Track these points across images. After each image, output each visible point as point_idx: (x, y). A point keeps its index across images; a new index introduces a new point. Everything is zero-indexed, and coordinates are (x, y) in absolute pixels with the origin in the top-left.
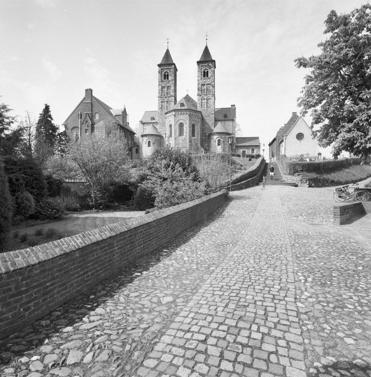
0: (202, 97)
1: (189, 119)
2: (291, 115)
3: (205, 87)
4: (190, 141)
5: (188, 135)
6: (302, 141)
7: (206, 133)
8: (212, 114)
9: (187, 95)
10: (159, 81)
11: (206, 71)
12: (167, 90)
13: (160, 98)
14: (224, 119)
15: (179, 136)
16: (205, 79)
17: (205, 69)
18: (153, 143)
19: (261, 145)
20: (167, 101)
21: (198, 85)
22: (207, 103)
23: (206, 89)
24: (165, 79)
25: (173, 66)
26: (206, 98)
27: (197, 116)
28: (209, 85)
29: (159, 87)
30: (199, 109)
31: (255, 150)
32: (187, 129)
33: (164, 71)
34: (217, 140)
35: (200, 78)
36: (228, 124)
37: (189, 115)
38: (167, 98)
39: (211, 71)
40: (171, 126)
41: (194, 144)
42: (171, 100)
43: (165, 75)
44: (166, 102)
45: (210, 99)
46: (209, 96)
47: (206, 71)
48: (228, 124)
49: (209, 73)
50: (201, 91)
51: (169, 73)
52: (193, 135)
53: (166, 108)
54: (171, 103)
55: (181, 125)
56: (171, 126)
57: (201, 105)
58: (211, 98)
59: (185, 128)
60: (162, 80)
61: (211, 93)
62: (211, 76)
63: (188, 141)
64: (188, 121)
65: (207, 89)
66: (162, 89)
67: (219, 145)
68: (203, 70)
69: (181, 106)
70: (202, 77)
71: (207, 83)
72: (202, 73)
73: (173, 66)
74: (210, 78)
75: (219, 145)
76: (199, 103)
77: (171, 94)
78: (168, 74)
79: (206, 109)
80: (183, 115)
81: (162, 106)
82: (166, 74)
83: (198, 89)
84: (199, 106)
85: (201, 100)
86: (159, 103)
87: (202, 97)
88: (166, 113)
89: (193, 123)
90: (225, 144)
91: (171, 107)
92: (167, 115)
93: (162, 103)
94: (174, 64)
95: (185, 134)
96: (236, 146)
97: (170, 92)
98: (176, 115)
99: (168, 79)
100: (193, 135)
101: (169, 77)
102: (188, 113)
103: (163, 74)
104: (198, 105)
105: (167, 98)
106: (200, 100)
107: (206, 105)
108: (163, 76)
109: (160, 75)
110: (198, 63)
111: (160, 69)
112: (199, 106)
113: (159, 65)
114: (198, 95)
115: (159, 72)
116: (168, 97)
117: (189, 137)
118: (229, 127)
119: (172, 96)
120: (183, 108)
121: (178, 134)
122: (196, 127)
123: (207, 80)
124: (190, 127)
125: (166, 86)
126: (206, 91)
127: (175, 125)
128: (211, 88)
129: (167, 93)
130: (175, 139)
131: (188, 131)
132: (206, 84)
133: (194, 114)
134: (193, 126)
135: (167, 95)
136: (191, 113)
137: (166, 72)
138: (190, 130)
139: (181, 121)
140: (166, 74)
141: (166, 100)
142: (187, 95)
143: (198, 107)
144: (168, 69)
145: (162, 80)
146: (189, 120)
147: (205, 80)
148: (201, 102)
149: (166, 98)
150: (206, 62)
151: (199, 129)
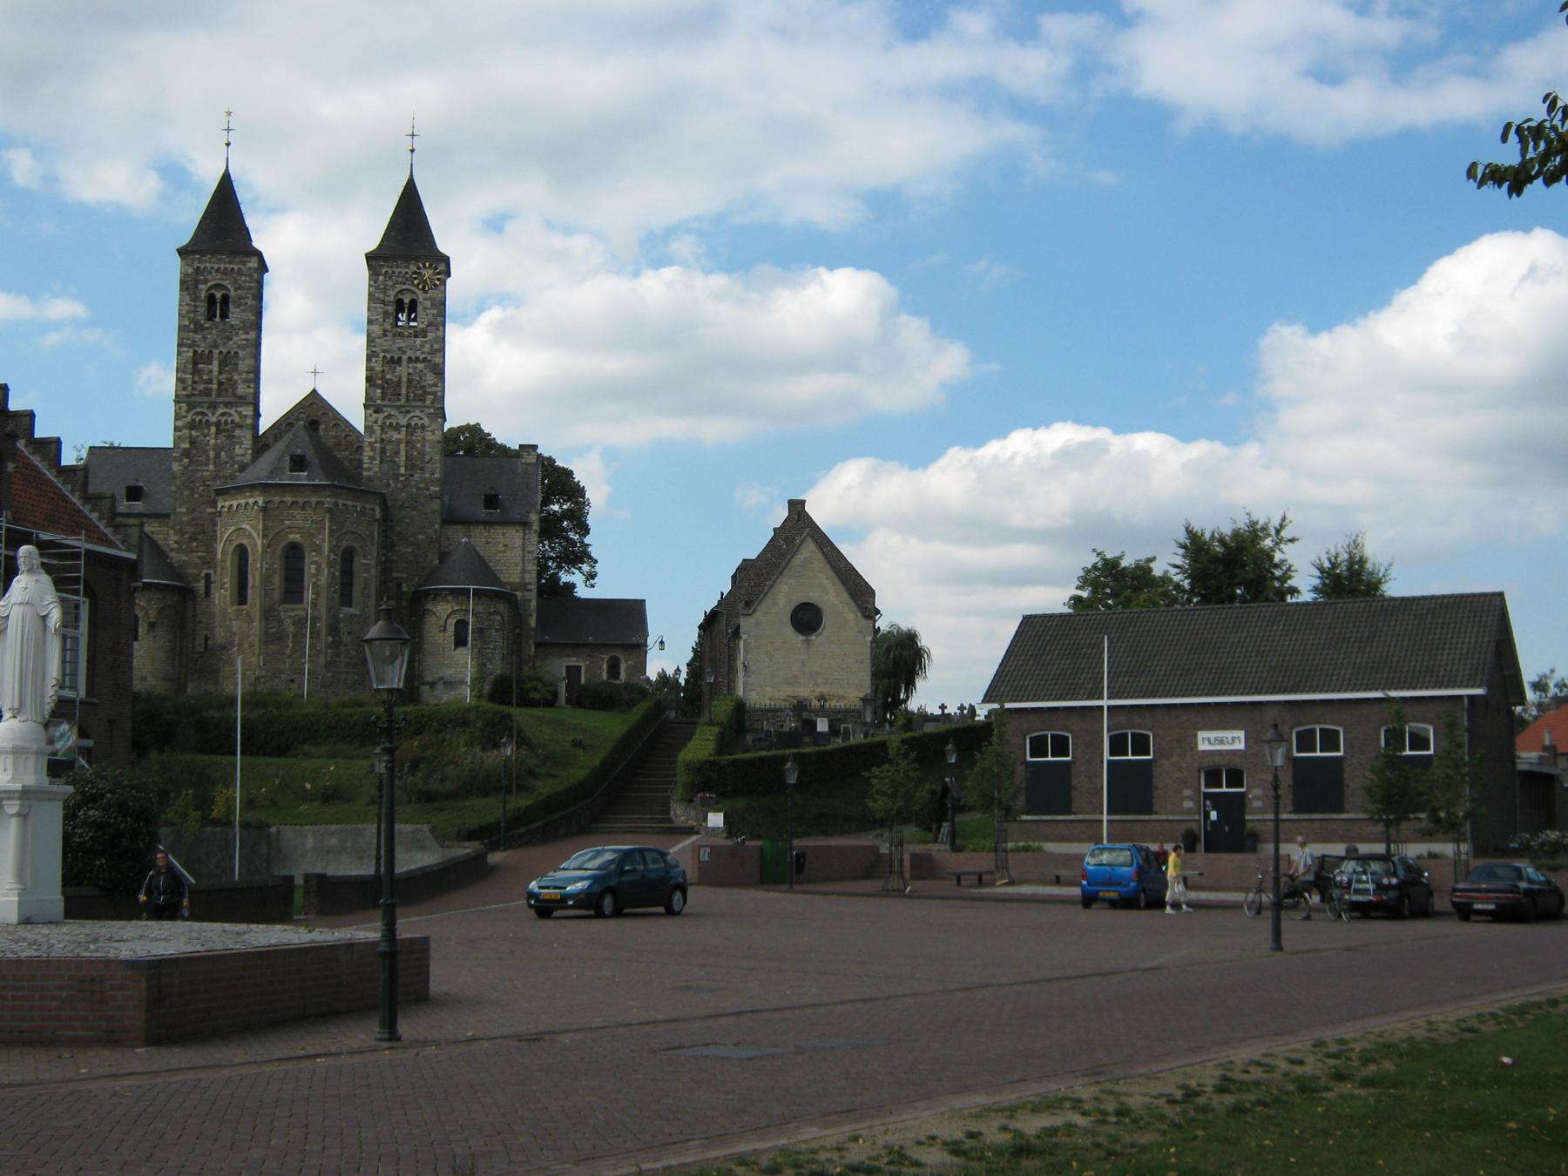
0: (389, 416)
1: (331, 530)
2: (782, 513)
3: (402, 371)
4: (333, 629)
5: (323, 602)
6: (813, 638)
7: (399, 585)
8: (432, 497)
9: (314, 391)
10: (182, 328)
11: (407, 301)
12: (220, 373)
13: (184, 406)
14: (483, 512)
15: (284, 601)
16: (401, 335)
17: (401, 292)
18: (152, 625)
19: (650, 642)
20: (218, 424)
21: (369, 358)
22: (407, 443)
23: (404, 379)
24: (211, 317)
25: (253, 264)
26: (404, 422)
27: (363, 512)
28: (420, 366)
29: (179, 354)
30: (368, 469)
31: (623, 666)
32: (318, 571)
33: (206, 281)
34: (452, 622)
35: (377, 329)
36: (500, 539)
37: (329, 511)
38: (221, 411)
39: (428, 304)
40: (242, 553)
41: (346, 639)
42: (237, 420)
43: (211, 299)
44: (213, 429)
45: (423, 427)
46: (417, 413)
47: (407, 301)
48: (500, 539)
49: (420, 309)
50: (383, 388)
51: (232, 294)
52: (346, 599)
53: (212, 454)
54: (238, 432)
55: (294, 555)
56: (242, 553)
57: (383, 451)
58: (426, 421)
59: (310, 569)
60: (196, 323)
61: (428, 402)
62: (430, 324)
63: (322, 625)
64: (325, 540)
65: (410, 381)
66: (195, 363)
67: (460, 641)
68: (392, 293)
69: (291, 471)
70: (388, 327)
71: (409, 353)
72: (391, 309)
73: (253, 264)
74: (424, 333)
75: (460, 641)
76: (371, 444)
77: (241, 389)
78: (225, 298)
79: (402, 470)
80: (303, 508)
81: (192, 443)
82: (219, 295)
83: (368, 379)
84: (372, 458)
85: (382, 430)
86: (176, 429)
87: (389, 416)
88: (219, 492)
89: (345, 543)
90: (486, 643)
91: (238, 451)
92: (223, 503)
93: (192, 429)
94: (259, 255)
95: (309, 595)
96: (538, 645)
97: (234, 384)
98: (270, 506)
99: (224, 316)
100: (346, 599)
101: (232, 308)
102: (328, 501)
103: (203, 295)
104: (367, 452)
105: (221, 411)
106: (377, 428)
107: (403, 453)
108: (203, 308)
109: (187, 299)
110: (370, 257)
111: (190, 270)
112: (372, 458)
113: (182, 252)
114: (366, 406)
115: (182, 283)
116: (227, 404)
117: (329, 610)
118: (509, 553)
119: (242, 400)
120: (303, 478)
121: (277, 594)
122: (359, 561)
123: (409, 341)
124: (331, 565)
125: (216, 352)
126: (404, 390)
127: (264, 552)
128: (430, 379)
129: (220, 384)
130: (268, 614)
131: (324, 579)
132: (405, 357)
133: (350, 503)
134: (347, 559)
135: (219, 395)
136: (340, 502)
137: (217, 286)
138: (332, 575)
139: (296, 537)
140: (219, 295)
141: (213, 419)
142: (314, 391)
143: (366, 460)
144: (226, 272)
145: (196, 323)
146: (331, 535)
147: (400, 343)
148: (382, 440)
149: (213, 407)
150: (408, 259)
151: (373, 571)
